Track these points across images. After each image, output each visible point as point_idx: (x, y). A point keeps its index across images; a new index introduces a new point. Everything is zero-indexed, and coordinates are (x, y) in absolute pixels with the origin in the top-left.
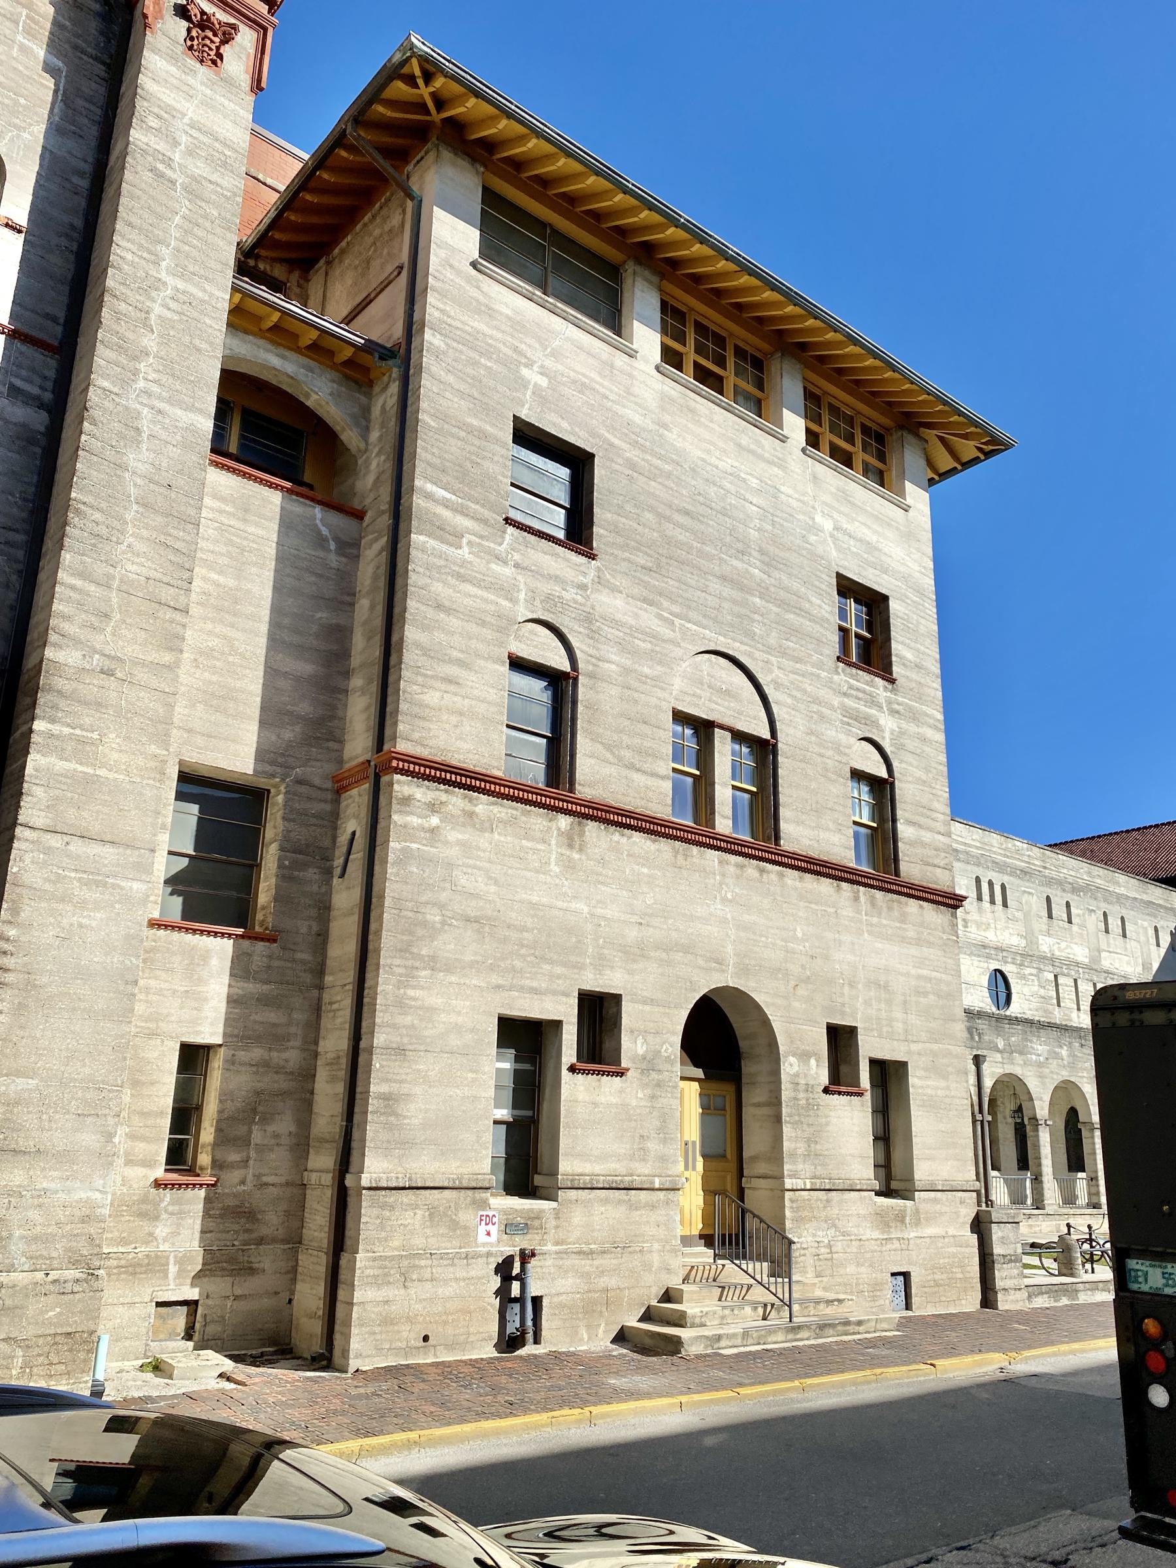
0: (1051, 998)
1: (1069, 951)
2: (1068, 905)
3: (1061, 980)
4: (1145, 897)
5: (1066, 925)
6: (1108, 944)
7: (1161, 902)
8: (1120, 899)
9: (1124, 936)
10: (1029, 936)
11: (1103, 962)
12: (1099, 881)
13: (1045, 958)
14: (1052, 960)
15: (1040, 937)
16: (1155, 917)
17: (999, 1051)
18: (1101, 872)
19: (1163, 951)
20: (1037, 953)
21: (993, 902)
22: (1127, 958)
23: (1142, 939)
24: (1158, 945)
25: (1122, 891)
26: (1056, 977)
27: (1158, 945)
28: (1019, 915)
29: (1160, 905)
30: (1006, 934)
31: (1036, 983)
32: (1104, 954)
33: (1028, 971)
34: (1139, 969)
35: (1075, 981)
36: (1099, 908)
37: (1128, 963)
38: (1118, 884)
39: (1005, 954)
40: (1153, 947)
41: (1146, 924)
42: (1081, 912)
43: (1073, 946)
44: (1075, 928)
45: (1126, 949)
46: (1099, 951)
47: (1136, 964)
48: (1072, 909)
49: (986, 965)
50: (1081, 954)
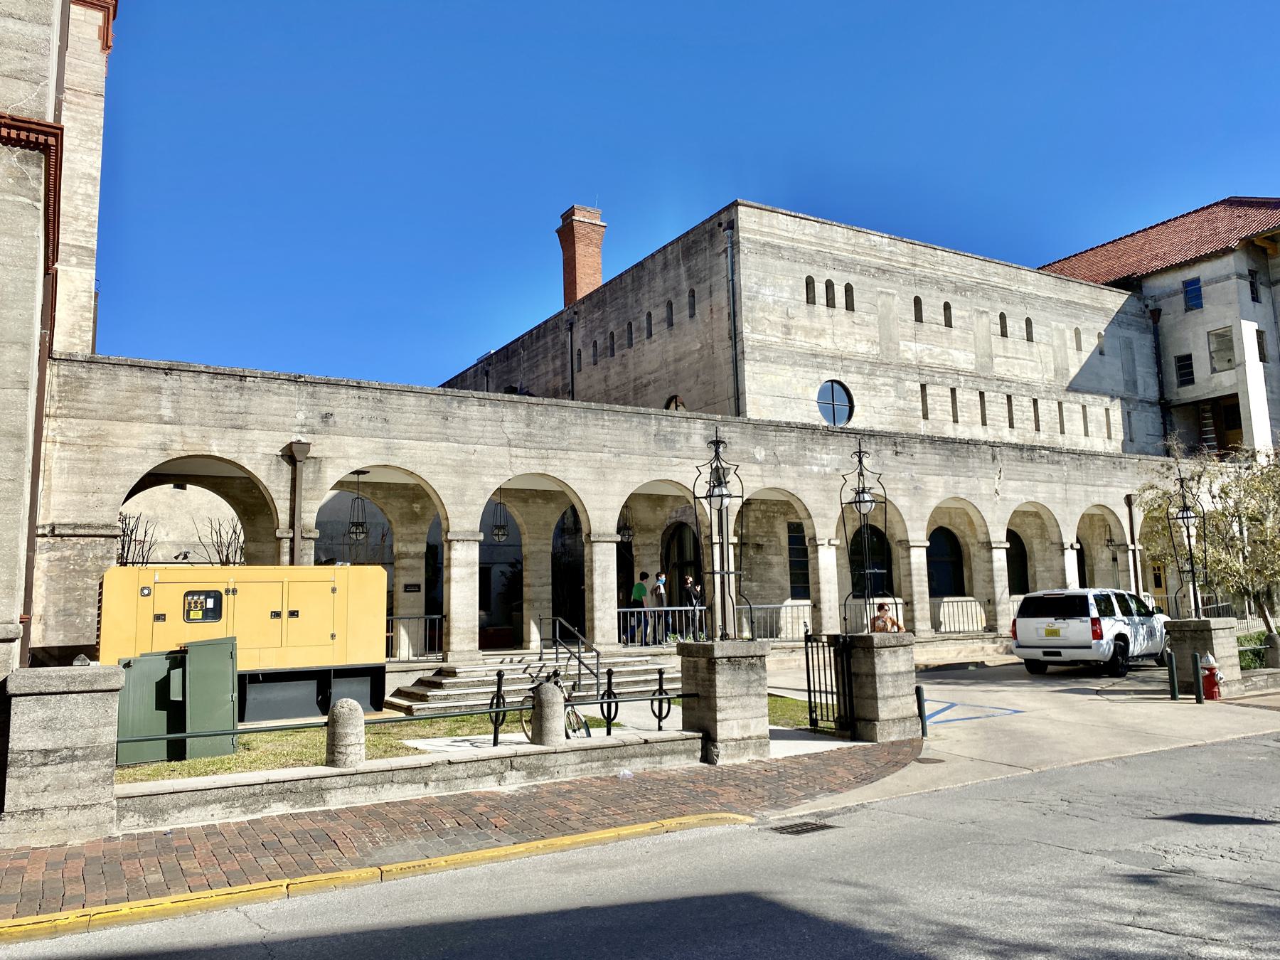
0: (915, 409)
1: (943, 357)
2: (947, 307)
3: (929, 390)
4: (1064, 297)
5: (943, 329)
6: (1005, 348)
7: (1087, 302)
8: (1025, 298)
9: (1030, 338)
10: (886, 340)
11: (996, 369)
12: (996, 279)
13: (908, 366)
14: (919, 368)
15: (902, 343)
16: (1077, 317)
17: (756, 462)
18: (1000, 269)
19: (1085, 356)
20: (895, 361)
21: (831, 303)
22: (1032, 364)
23: (1056, 342)
24: (1079, 348)
25: (1031, 289)
26: (923, 387)
27: (1079, 348)
28: (871, 318)
29: (1085, 306)
30: (850, 341)
31: (893, 393)
32: (996, 360)
33: (880, 381)
34: (1050, 375)
35: (953, 391)
36: (994, 309)
37: (1034, 369)
38: (1026, 283)
39: (846, 363)
40: (1072, 352)
41: (1062, 326)
42: (966, 314)
43: (950, 351)
44: (955, 332)
45: (1031, 354)
46: (991, 357)
47: (1045, 370)
48: (953, 311)
49: (816, 376)
50: (964, 359)
